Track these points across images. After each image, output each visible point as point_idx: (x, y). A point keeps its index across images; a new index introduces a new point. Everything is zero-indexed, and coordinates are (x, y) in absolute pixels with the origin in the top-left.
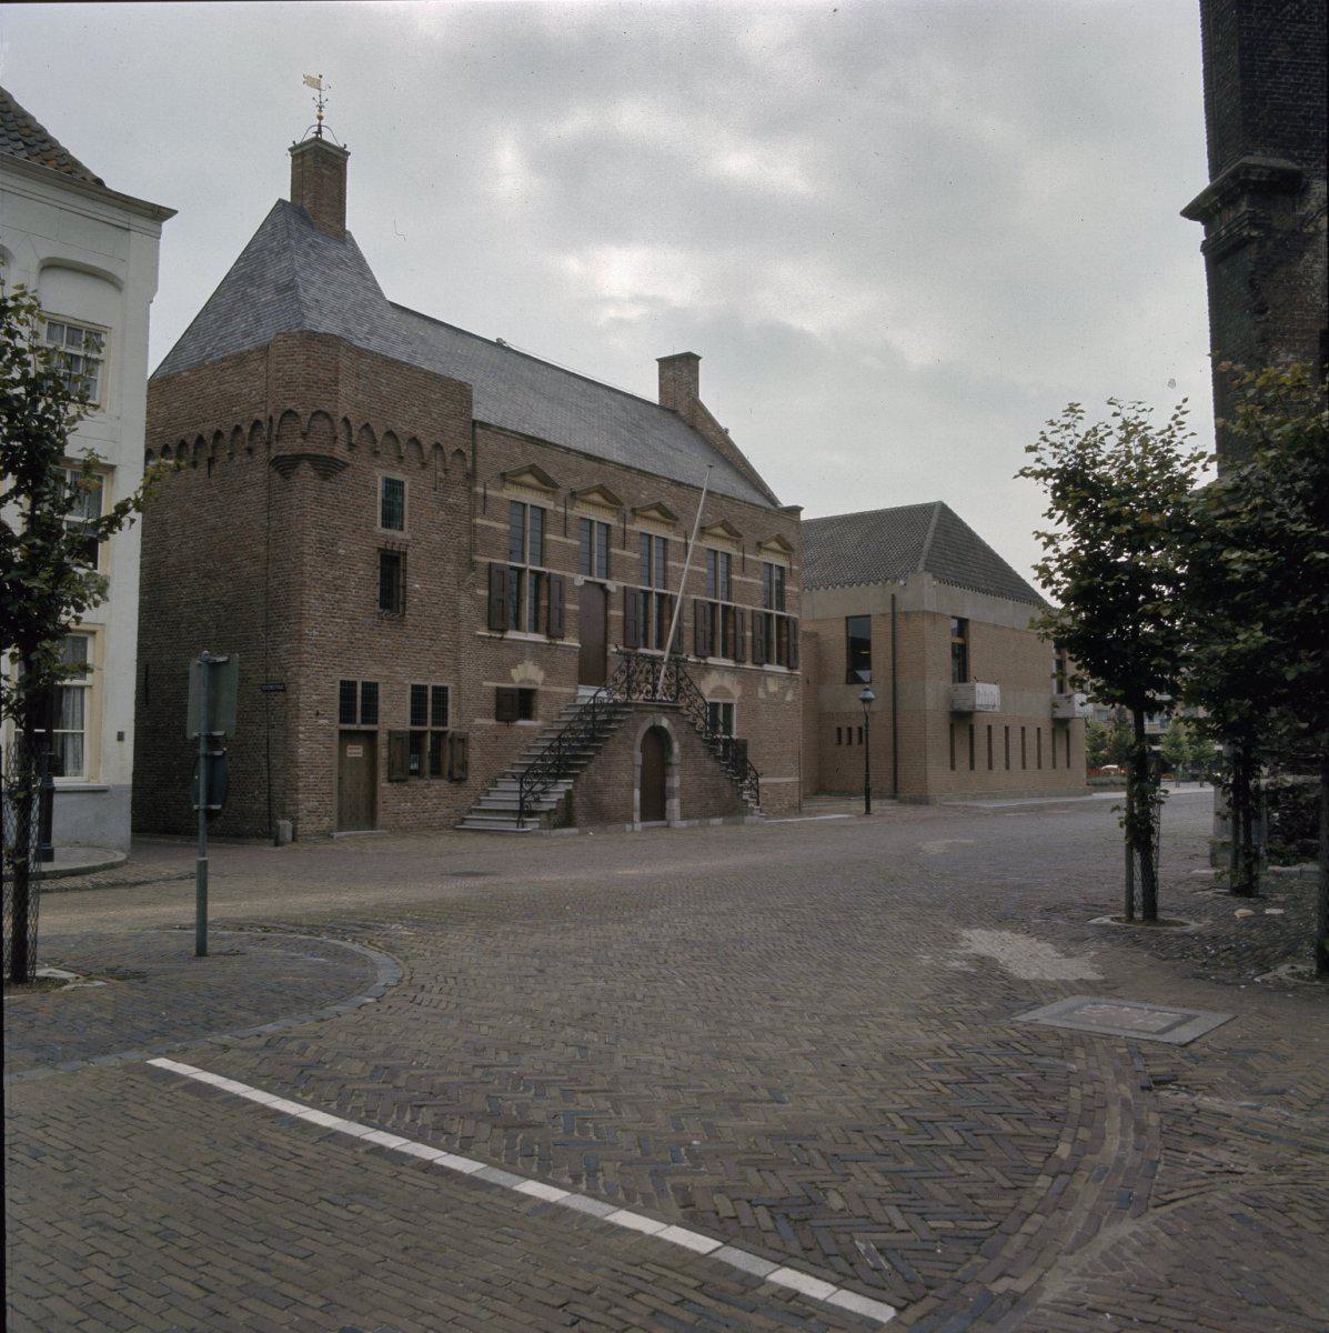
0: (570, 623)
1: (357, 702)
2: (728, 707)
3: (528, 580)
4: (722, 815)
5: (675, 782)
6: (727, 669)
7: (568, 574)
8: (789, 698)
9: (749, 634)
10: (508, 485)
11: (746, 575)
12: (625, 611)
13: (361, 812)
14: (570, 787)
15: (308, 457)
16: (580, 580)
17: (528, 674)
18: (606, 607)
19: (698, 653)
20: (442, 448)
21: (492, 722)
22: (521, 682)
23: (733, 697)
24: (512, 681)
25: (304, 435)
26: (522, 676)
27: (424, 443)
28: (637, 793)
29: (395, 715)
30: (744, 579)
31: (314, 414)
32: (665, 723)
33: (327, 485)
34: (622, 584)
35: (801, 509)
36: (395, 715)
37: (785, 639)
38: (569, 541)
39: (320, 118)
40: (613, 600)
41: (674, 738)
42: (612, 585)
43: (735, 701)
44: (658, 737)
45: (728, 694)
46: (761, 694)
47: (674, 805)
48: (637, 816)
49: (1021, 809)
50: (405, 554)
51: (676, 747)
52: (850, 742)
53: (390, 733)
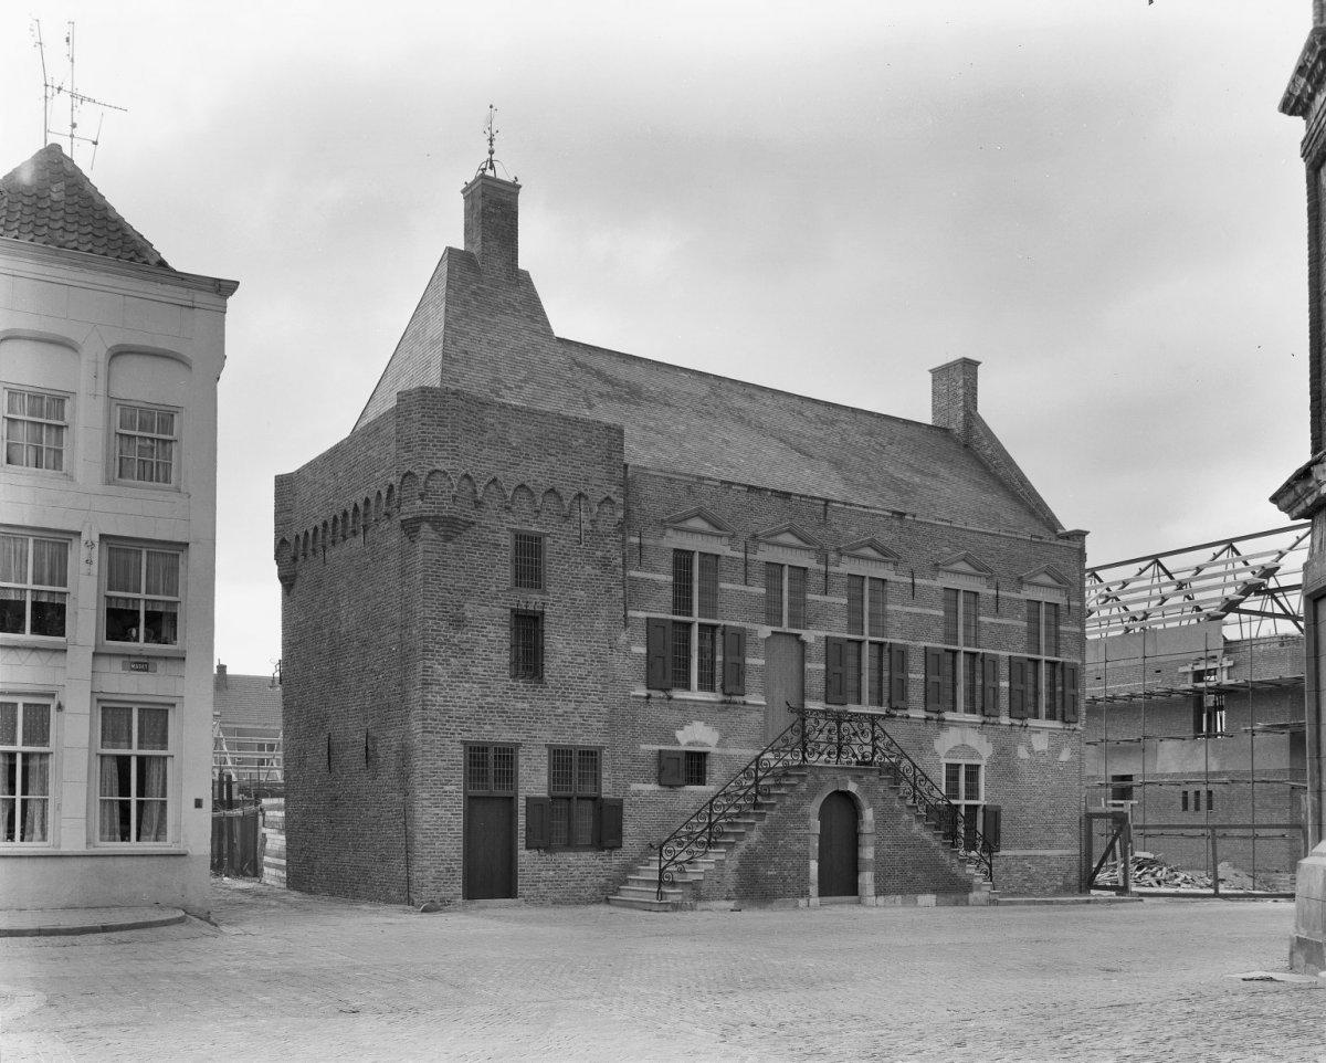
0: (752, 681)
1: (489, 766)
2: (972, 771)
4: (934, 891)
5: (868, 853)
6: (972, 725)
7: (748, 626)
8: (1065, 756)
9: (1005, 684)
11: (1002, 616)
12: (826, 664)
13: (489, 878)
14: (722, 857)
15: (427, 519)
16: (765, 631)
17: (696, 735)
18: (803, 659)
19: (928, 708)
20: (587, 498)
21: (653, 787)
22: (690, 744)
23: (981, 758)
24: (677, 743)
25: (422, 496)
26: (691, 739)
27: (563, 493)
28: (814, 866)
29: (533, 781)
31: (432, 473)
33: (450, 546)
34: (823, 634)
35: (1087, 533)
36: (533, 781)
37: (1059, 689)
38: (750, 589)
40: (811, 652)
42: (809, 636)
43: (983, 763)
45: (974, 753)
46: (1022, 753)
47: (867, 879)
48: (814, 890)
49: (1073, 903)
50: (543, 613)
51: (868, 815)
52: (1197, 808)
53: (527, 799)
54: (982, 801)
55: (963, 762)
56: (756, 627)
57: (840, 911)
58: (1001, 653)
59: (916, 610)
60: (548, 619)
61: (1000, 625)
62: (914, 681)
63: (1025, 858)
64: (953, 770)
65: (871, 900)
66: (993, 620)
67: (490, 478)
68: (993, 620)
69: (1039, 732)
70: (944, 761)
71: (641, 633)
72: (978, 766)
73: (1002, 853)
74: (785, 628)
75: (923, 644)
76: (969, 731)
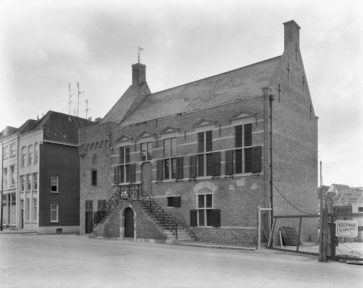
2: (209, 197)
3: (125, 167)
4: (154, 238)
6: (208, 180)
7: (136, 163)
8: (254, 187)
10: (139, 140)
11: (222, 137)
23: (212, 192)
30: (220, 139)
32: (130, 206)
33: (83, 160)
38: (137, 152)
39: (139, 57)
41: (134, 211)
43: (213, 194)
44: (128, 210)
45: (209, 190)
46: (231, 188)
51: (135, 213)
54: (213, 208)
55: (205, 194)
56: (138, 162)
57: (127, 241)
58: (221, 151)
59: (187, 144)
60: (98, 171)
61: (221, 140)
62: (186, 168)
63: (232, 229)
64: (201, 197)
65: (135, 239)
66: (218, 139)
67: (87, 144)
68: (218, 139)
69: (239, 179)
70: (197, 194)
71: (113, 170)
72: (211, 195)
73: (221, 227)
74: (147, 161)
75: (189, 155)
76: (207, 182)
